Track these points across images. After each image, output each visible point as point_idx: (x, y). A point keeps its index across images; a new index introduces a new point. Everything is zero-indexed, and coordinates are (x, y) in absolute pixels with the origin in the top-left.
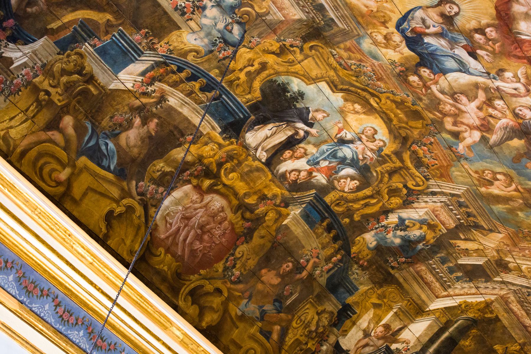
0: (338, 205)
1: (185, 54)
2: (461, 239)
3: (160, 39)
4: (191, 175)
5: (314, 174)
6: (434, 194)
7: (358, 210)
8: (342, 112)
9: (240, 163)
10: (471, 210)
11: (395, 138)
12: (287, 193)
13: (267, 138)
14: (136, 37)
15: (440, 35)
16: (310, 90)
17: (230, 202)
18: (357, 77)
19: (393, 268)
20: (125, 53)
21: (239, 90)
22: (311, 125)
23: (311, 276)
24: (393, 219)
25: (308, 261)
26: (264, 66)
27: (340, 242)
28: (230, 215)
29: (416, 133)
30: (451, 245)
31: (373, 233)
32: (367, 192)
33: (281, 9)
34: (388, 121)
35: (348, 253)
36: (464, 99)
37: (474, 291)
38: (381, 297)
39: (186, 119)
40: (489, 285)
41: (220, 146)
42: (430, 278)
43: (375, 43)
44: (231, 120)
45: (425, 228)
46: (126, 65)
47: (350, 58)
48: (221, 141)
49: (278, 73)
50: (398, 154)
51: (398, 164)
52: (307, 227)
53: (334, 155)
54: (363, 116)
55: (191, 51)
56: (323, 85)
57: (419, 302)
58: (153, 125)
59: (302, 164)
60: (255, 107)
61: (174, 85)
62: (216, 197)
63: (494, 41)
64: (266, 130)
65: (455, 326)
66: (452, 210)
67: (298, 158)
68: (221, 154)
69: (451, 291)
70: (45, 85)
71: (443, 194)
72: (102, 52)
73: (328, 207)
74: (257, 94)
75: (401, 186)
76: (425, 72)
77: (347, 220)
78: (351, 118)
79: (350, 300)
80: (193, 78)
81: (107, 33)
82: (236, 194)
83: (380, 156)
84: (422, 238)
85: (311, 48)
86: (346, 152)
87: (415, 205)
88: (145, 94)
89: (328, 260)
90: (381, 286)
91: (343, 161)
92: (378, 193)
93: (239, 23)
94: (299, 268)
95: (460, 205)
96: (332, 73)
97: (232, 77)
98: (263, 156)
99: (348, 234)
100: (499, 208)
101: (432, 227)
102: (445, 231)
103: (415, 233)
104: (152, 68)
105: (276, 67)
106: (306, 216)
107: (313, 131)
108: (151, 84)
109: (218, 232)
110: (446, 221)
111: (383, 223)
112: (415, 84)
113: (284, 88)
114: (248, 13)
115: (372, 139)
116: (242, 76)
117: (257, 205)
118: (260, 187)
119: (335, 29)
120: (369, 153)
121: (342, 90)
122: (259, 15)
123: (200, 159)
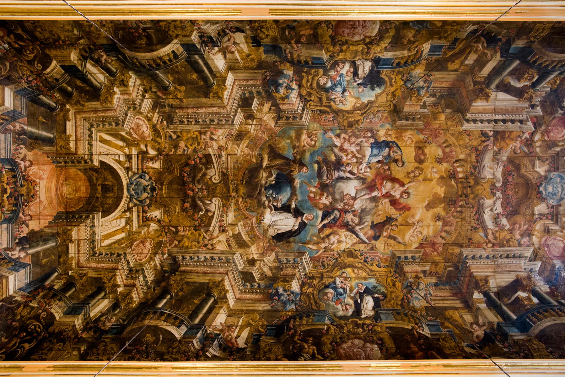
0: (316, 72)
1: (415, 66)
2: (271, 107)
3: (427, 64)
4: (376, 39)
5: (336, 73)
6: (303, 109)
7: (307, 77)
8: (358, 98)
9: (363, 54)
10: (291, 120)
11: (339, 110)
12: (336, 59)
13: (364, 68)
14: (434, 58)
15: (389, 155)
16: (373, 93)
17: (352, 41)
18: (373, 113)
19: (266, 72)
20: (433, 52)
21: (389, 72)
22: (358, 84)
23: (290, 43)
24: (294, 86)
25: (298, 47)
26: (391, 85)
27: (296, 62)
28: (347, 38)
29: (341, 120)
30: (269, 101)
31: (292, 75)
32: (315, 85)
33: (410, 105)
34: (348, 112)
35: (288, 61)
36: (358, 148)
37: (233, 96)
38: (252, 60)
39: (395, 51)
40: (235, 105)
41: (375, 53)
42: (250, 82)
43: (388, 130)
44: (381, 63)
45: (284, 96)
46: (430, 49)
47: (382, 116)
48: (378, 55)
49: (386, 88)
50: (330, 107)
51: (324, 104)
52: (314, 56)
53: (340, 84)
54: (353, 104)
55: (414, 69)
56: (373, 99)
57: (237, 71)
58: (405, 41)
59: (344, 71)
60: (379, 72)
61: (409, 57)
62: (359, 39)
63: (384, 172)
64: (367, 70)
65: (211, 78)
66: (291, 112)
67: (347, 72)
68: (372, 51)
69: (236, 87)
70: (455, 28)
71: (303, 113)
72: (441, 47)
73: (317, 67)
74: (383, 76)
75: (312, 99)
76: (372, 140)
77: (305, 70)
78: (354, 100)
79: (262, 49)
80: (406, 63)
81: (444, 52)
82: (352, 45)
83: (331, 99)
84: (277, 92)
85: (390, 105)
86: (339, 89)
87: (299, 99)
88: (416, 47)
89: (291, 53)
90: (258, 62)
91: (335, 85)
92: (312, 88)
93: (412, 89)
94: (297, 42)
95: (295, 118)
96: (377, 105)
97: (395, 74)
98: (358, 62)
99: (298, 67)
100: (293, 134)
101: (283, 99)
102: (278, 102)
103: (282, 91)
104: (421, 55)
105: (389, 89)
106: (320, 59)
107: (355, 84)
108: (417, 51)
109: (346, 31)
110: (284, 106)
111: (294, 82)
112: (366, 133)
113: (379, 86)
114: (414, 94)
115: (341, 102)
116: (393, 77)
117: (341, 48)
118: (347, 53)
119: (397, 119)
120: (334, 96)
121: (368, 104)
122: (411, 97)
123: (378, 45)
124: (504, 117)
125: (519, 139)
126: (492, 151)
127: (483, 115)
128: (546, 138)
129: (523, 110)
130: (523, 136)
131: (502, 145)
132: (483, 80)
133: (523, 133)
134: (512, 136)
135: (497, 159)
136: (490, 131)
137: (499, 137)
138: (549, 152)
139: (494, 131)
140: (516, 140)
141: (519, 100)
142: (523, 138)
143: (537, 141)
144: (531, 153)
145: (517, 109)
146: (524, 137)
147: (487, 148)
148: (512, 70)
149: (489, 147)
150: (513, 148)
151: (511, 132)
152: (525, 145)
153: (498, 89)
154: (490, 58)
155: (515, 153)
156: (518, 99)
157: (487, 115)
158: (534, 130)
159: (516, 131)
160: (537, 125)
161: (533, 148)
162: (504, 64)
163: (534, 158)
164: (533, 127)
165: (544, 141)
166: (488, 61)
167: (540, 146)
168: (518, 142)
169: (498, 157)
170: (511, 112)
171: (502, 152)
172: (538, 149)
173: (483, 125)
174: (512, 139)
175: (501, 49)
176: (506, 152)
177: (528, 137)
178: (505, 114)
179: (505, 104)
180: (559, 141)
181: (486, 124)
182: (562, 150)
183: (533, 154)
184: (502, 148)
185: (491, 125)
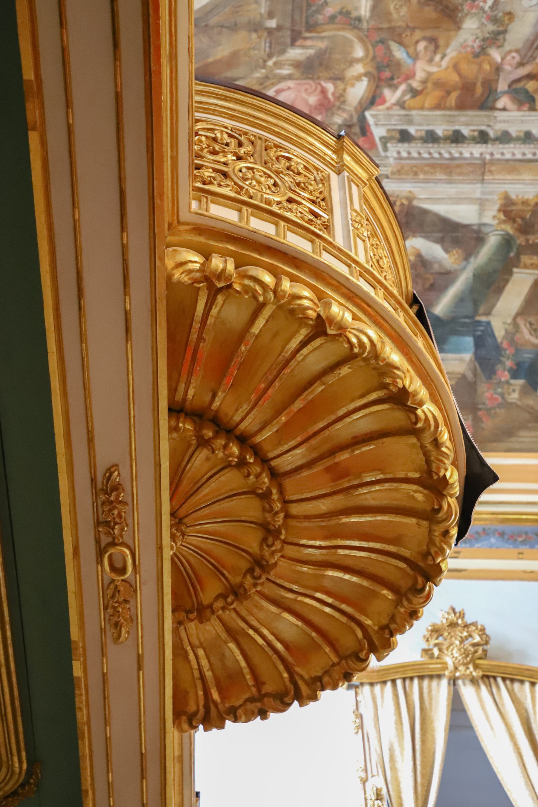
124: (455, 150)
125: (415, 84)
126: (507, 47)
127: (519, 156)
128: (330, 87)
129: (399, 172)
130: (404, 94)
131: (474, 68)
132: (525, 259)
133: (401, 104)
134: (439, 93)
135: (495, 20)
136: (504, 109)
137: (479, 90)
138: (322, 45)
139: (493, 108)
140: (424, 82)
141: (410, 199)
142: (403, 87)
143: (358, 78)
144: (382, 41)
145: (416, 174)
146: (399, 93)
147: (522, 58)
148: (444, 288)
149: (518, 58)
150: (438, 58)
151: (438, 107)
152: (399, 64)
153: (479, 232)
154: (521, 322)
155: (433, 40)
156: (415, 203)
157: (508, 156)
158: (367, 114)
159: (422, 108)
160: (356, 130)
161: (374, 58)
162: (476, 304)
163: (373, 23)
164: (371, 120)
165: (338, 78)
166: (523, 312)
167: (352, 62)
168: (420, 75)
169: (491, 27)
170: (433, 166)
171: (477, 43)
172: (359, 52)
173: (526, 127)
174: (438, 84)
175: (498, 348)
176: (464, 46)
177: (387, 92)
178: (452, 158)
179: (451, 190)
180: (290, 77)
181: (513, 131)
182: (283, 52)
183: (377, 37)
184: (476, 55)
185: (500, 127)
